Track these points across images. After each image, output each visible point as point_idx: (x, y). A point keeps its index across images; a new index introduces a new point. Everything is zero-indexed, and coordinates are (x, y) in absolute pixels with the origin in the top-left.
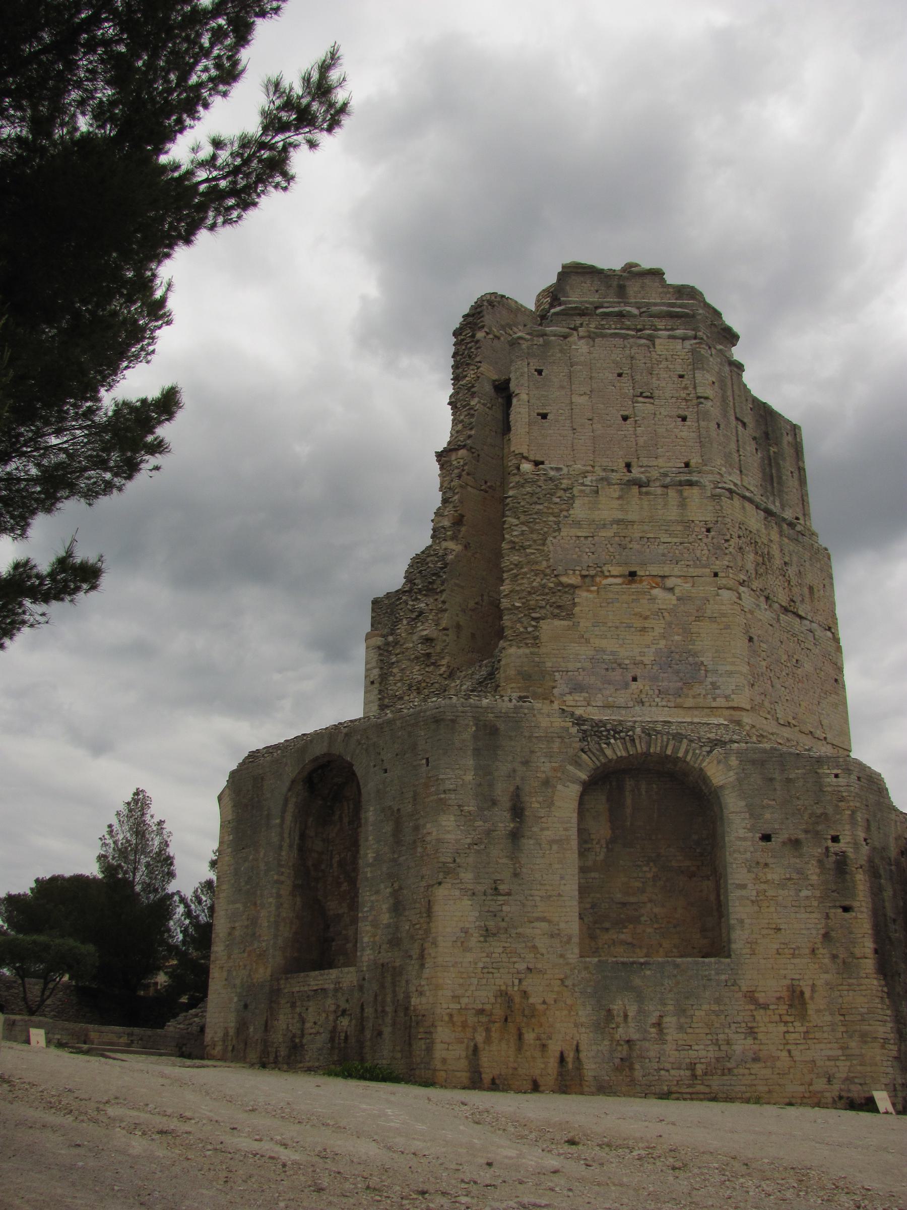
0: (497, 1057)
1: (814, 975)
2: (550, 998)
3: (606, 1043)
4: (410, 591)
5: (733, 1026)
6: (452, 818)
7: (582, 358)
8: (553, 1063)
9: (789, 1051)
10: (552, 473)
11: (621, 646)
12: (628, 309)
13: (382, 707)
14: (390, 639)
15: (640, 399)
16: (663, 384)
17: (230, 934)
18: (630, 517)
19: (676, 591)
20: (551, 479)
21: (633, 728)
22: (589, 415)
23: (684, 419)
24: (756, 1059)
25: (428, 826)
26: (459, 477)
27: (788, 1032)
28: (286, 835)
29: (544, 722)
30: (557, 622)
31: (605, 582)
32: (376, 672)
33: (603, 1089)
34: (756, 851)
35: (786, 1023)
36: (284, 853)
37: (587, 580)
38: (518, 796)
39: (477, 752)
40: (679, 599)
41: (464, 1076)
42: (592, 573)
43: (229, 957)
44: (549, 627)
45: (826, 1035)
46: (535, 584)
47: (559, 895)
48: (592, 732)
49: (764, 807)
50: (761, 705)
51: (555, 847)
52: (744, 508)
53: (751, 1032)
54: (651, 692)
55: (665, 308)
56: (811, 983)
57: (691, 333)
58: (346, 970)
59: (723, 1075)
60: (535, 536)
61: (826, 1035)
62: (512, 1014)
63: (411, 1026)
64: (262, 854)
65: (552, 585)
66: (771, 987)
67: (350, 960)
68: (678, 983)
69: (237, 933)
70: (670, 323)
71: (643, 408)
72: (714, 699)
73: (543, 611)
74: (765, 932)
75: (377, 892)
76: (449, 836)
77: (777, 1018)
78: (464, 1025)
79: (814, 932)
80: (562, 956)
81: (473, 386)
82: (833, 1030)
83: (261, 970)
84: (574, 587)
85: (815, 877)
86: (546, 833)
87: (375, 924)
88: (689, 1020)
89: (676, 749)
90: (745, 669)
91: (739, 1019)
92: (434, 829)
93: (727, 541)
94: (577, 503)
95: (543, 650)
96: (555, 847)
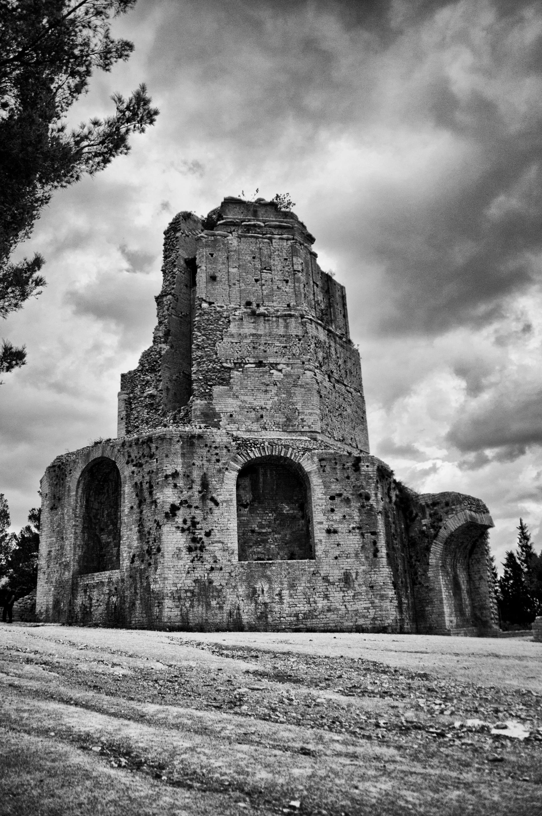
1: (357, 567)
2: (224, 583)
3: (253, 604)
4: (142, 370)
5: (317, 594)
6: (171, 490)
7: (234, 249)
9: (345, 605)
10: (218, 309)
11: (255, 400)
12: (259, 223)
13: (128, 432)
14: (131, 395)
15: (265, 271)
16: (276, 263)
17: (49, 554)
18: (259, 333)
19: (283, 371)
21: (264, 442)
22: (238, 278)
23: (287, 282)
24: (329, 610)
25: (158, 494)
26: (168, 310)
27: (345, 596)
28: (79, 501)
29: (218, 440)
30: (221, 387)
31: (246, 366)
32: (124, 413)
34: (327, 505)
35: (344, 591)
36: (78, 510)
37: (237, 365)
38: (205, 477)
39: (183, 455)
40: (284, 376)
42: (240, 361)
43: (48, 567)
45: (363, 597)
46: (210, 367)
47: (227, 529)
48: (244, 445)
49: (331, 483)
50: (326, 430)
51: (225, 504)
52: (317, 328)
53: (326, 597)
54: (270, 424)
56: (355, 571)
57: (291, 237)
58: (114, 571)
59: (313, 618)
60: (209, 342)
61: (363, 597)
62: (204, 591)
63: (152, 599)
64: (66, 511)
65: (218, 368)
66: (336, 574)
67: (116, 565)
68: (289, 573)
69: (52, 554)
70: (280, 231)
71: (266, 275)
72: (303, 427)
73: (214, 381)
74: (333, 546)
75: (131, 530)
76: (169, 499)
77: (339, 589)
79: (357, 545)
80: (229, 561)
81: (175, 262)
82: (367, 594)
83: (67, 573)
84: (230, 369)
85: (357, 518)
86: (220, 497)
87: (130, 547)
88: (295, 592)
89: (286, 453)
90: (318, 412)
91: (320, 590)
92: (161, 496)
93: (309, 346)
94: (232, 325)
95: (214, 401)
96: (225, 504)
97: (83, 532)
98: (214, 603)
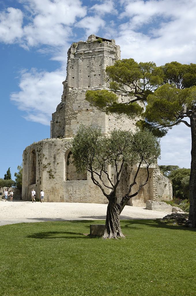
0: (51, 197)
8: (59, 198)
15: (92, 72)
20: (74, 92)
23: (100, 75)
28: (30, 162)
32: (52, 128)
33: (67, 201)
41: (46, 200)
44: (73, 121)
55: (97, 50)
62: (53, 190)
70: (98, 53)
71: (93, 73)
78: (47, 192)
84: (77, 113)
97: (32, 172)
98: (56, 193)
